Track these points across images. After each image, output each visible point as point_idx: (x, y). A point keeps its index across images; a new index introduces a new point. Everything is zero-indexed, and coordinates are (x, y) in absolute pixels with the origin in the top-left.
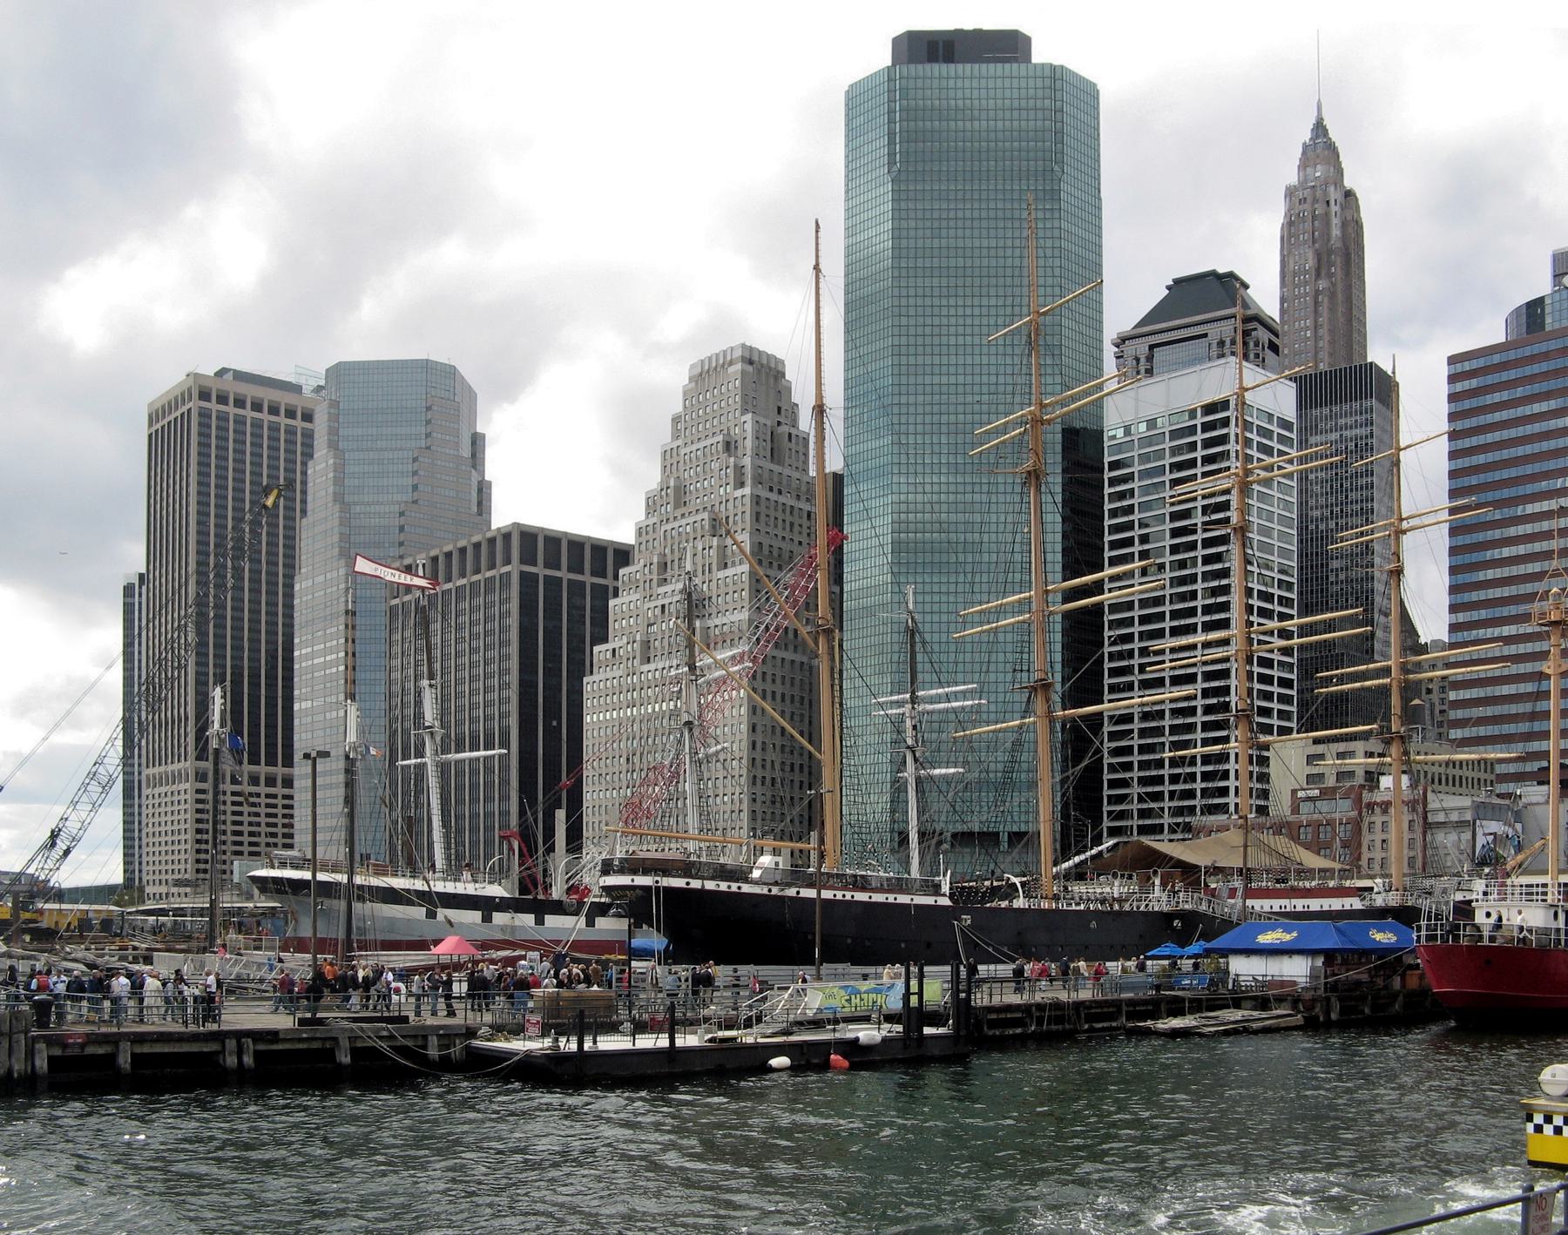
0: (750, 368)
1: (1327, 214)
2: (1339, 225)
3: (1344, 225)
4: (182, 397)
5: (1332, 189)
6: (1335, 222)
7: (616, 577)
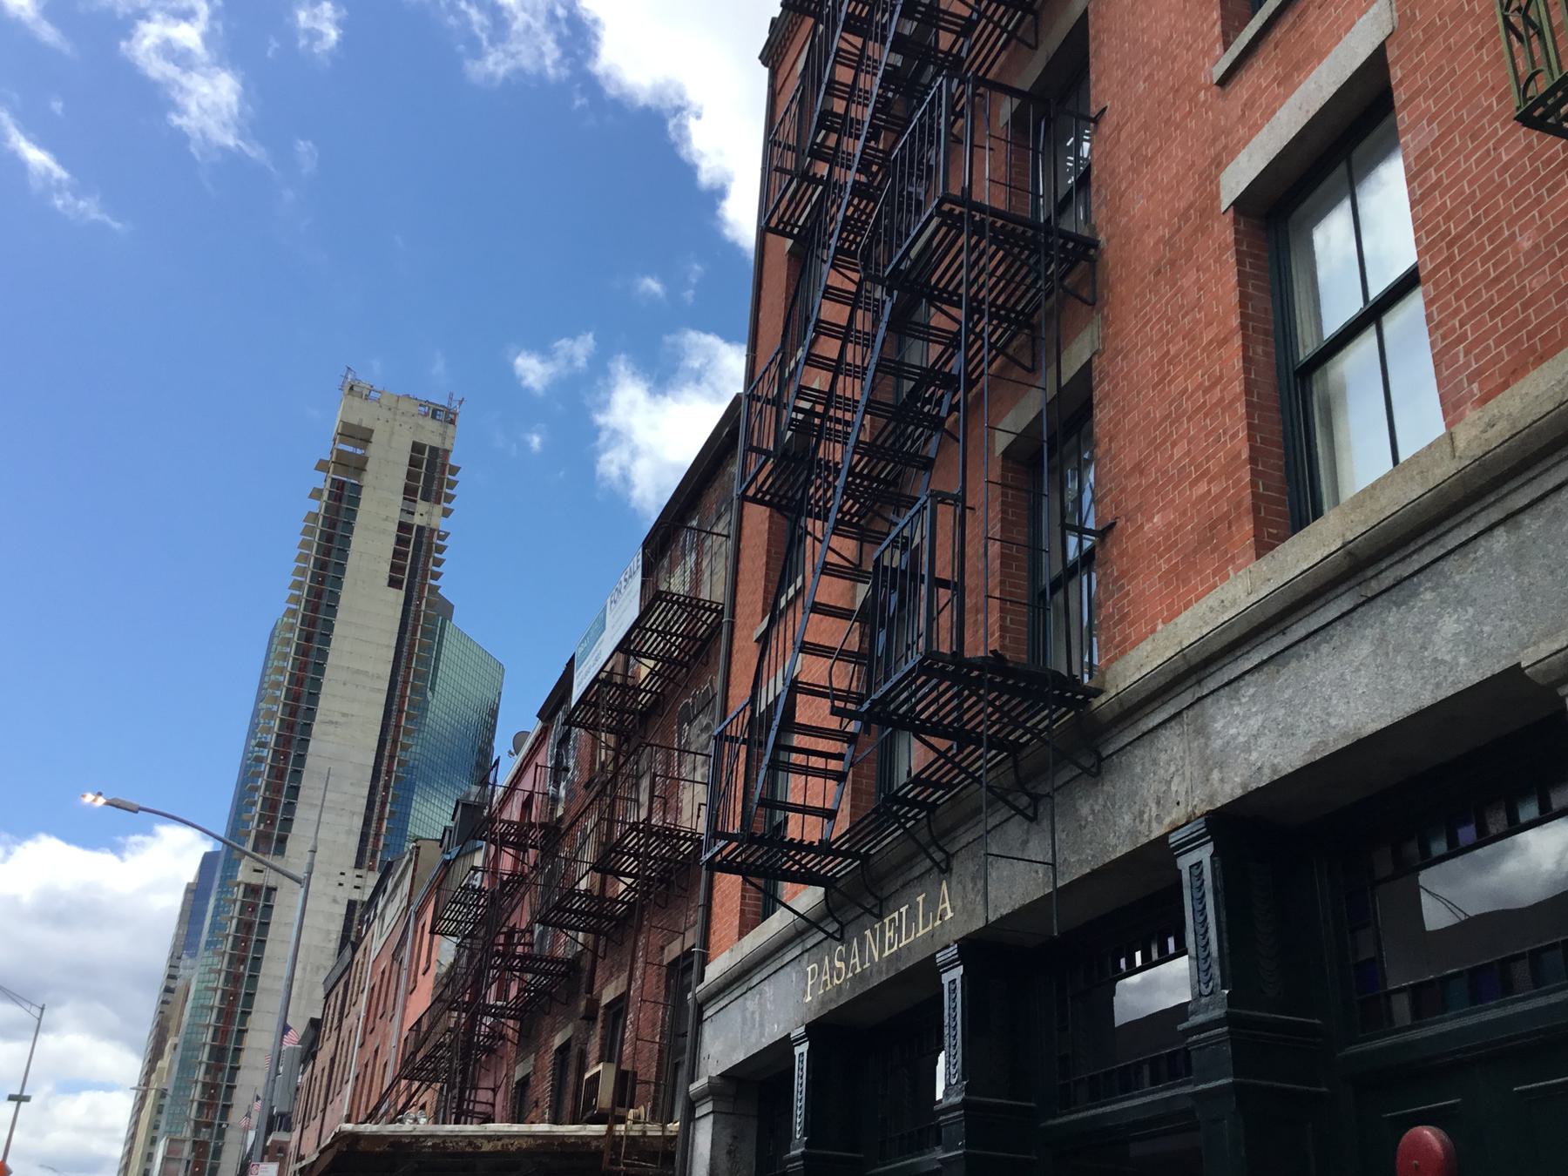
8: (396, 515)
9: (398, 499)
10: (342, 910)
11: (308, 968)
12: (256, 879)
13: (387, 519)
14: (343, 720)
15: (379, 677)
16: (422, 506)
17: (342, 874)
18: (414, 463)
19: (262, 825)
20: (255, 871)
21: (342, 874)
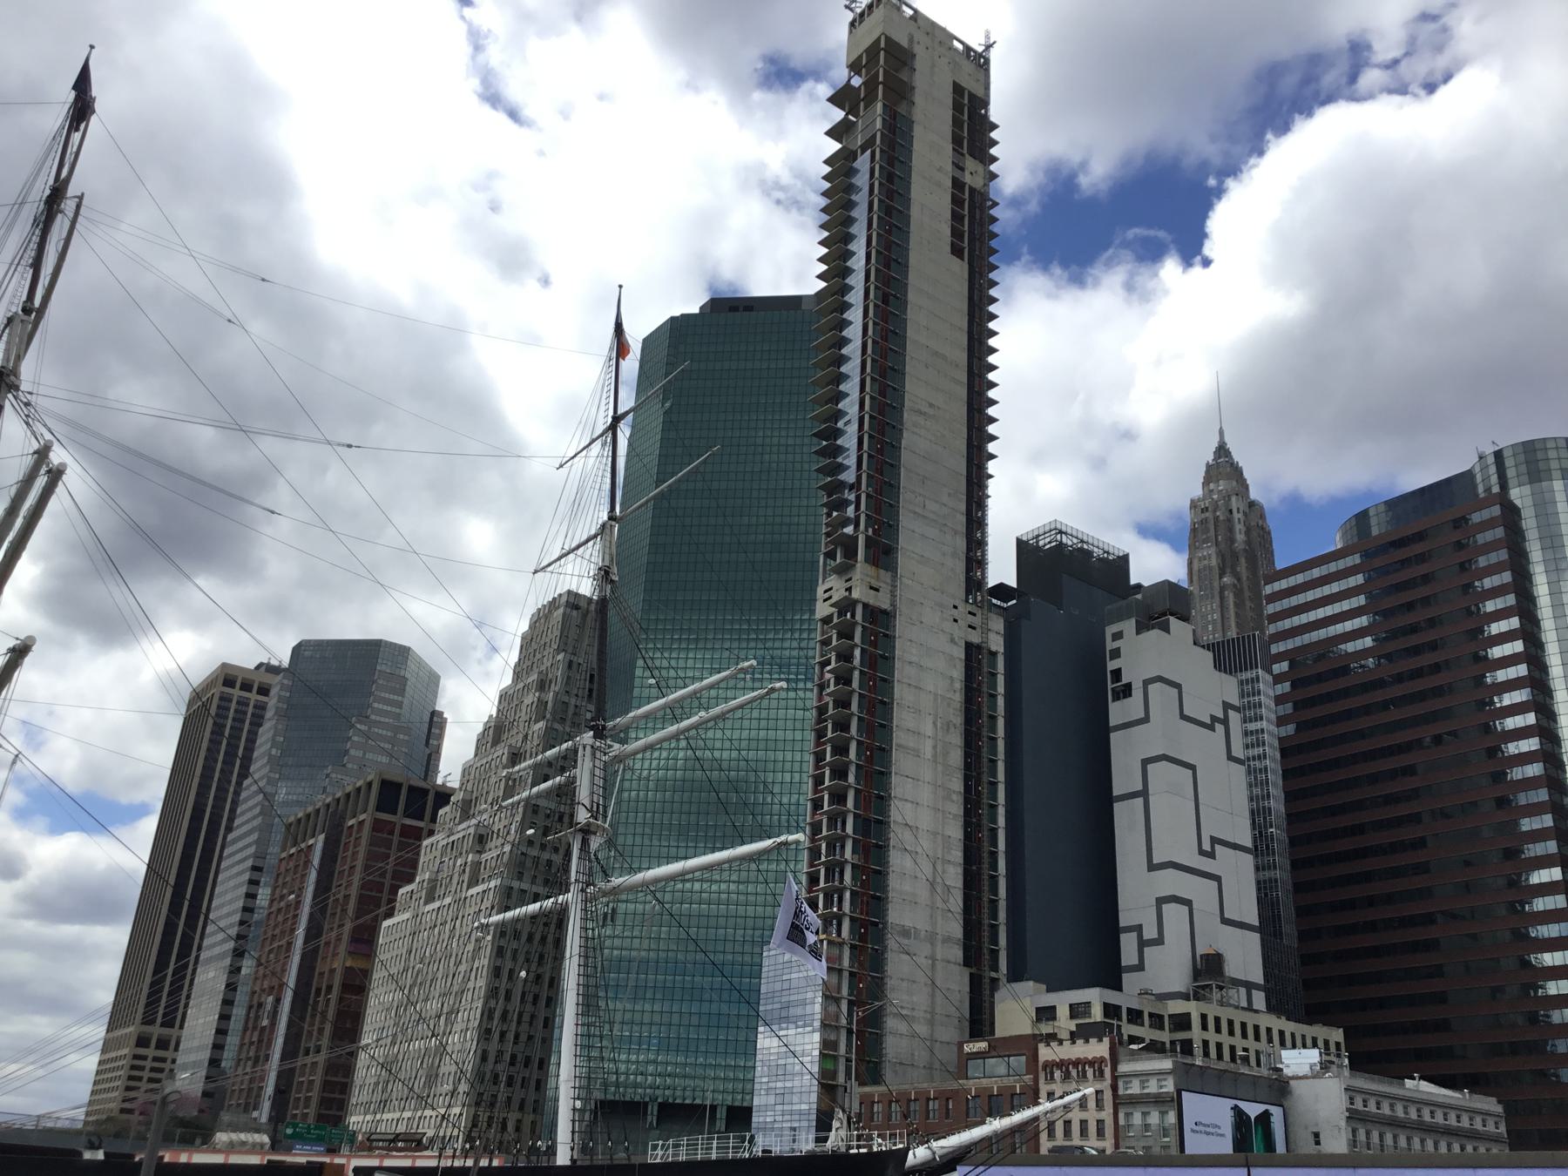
0: (575, 613)
1: (1230, 520)
2: (1244, 529)
3: (1248, 532)
4: (210, 683)
6: (1239, 527)
7: (434, 819)
8: (949, 167)
9: (949, 147)
10: (960, 653)
11: (939, 725)
13: (940, 170)
14: (931, 411)
15: (957, 366)
16: (970, 164)
17: (955, 607)
18: (957, 107)
19: (870, 530)
20: (871, 588)
21: (955, 607)
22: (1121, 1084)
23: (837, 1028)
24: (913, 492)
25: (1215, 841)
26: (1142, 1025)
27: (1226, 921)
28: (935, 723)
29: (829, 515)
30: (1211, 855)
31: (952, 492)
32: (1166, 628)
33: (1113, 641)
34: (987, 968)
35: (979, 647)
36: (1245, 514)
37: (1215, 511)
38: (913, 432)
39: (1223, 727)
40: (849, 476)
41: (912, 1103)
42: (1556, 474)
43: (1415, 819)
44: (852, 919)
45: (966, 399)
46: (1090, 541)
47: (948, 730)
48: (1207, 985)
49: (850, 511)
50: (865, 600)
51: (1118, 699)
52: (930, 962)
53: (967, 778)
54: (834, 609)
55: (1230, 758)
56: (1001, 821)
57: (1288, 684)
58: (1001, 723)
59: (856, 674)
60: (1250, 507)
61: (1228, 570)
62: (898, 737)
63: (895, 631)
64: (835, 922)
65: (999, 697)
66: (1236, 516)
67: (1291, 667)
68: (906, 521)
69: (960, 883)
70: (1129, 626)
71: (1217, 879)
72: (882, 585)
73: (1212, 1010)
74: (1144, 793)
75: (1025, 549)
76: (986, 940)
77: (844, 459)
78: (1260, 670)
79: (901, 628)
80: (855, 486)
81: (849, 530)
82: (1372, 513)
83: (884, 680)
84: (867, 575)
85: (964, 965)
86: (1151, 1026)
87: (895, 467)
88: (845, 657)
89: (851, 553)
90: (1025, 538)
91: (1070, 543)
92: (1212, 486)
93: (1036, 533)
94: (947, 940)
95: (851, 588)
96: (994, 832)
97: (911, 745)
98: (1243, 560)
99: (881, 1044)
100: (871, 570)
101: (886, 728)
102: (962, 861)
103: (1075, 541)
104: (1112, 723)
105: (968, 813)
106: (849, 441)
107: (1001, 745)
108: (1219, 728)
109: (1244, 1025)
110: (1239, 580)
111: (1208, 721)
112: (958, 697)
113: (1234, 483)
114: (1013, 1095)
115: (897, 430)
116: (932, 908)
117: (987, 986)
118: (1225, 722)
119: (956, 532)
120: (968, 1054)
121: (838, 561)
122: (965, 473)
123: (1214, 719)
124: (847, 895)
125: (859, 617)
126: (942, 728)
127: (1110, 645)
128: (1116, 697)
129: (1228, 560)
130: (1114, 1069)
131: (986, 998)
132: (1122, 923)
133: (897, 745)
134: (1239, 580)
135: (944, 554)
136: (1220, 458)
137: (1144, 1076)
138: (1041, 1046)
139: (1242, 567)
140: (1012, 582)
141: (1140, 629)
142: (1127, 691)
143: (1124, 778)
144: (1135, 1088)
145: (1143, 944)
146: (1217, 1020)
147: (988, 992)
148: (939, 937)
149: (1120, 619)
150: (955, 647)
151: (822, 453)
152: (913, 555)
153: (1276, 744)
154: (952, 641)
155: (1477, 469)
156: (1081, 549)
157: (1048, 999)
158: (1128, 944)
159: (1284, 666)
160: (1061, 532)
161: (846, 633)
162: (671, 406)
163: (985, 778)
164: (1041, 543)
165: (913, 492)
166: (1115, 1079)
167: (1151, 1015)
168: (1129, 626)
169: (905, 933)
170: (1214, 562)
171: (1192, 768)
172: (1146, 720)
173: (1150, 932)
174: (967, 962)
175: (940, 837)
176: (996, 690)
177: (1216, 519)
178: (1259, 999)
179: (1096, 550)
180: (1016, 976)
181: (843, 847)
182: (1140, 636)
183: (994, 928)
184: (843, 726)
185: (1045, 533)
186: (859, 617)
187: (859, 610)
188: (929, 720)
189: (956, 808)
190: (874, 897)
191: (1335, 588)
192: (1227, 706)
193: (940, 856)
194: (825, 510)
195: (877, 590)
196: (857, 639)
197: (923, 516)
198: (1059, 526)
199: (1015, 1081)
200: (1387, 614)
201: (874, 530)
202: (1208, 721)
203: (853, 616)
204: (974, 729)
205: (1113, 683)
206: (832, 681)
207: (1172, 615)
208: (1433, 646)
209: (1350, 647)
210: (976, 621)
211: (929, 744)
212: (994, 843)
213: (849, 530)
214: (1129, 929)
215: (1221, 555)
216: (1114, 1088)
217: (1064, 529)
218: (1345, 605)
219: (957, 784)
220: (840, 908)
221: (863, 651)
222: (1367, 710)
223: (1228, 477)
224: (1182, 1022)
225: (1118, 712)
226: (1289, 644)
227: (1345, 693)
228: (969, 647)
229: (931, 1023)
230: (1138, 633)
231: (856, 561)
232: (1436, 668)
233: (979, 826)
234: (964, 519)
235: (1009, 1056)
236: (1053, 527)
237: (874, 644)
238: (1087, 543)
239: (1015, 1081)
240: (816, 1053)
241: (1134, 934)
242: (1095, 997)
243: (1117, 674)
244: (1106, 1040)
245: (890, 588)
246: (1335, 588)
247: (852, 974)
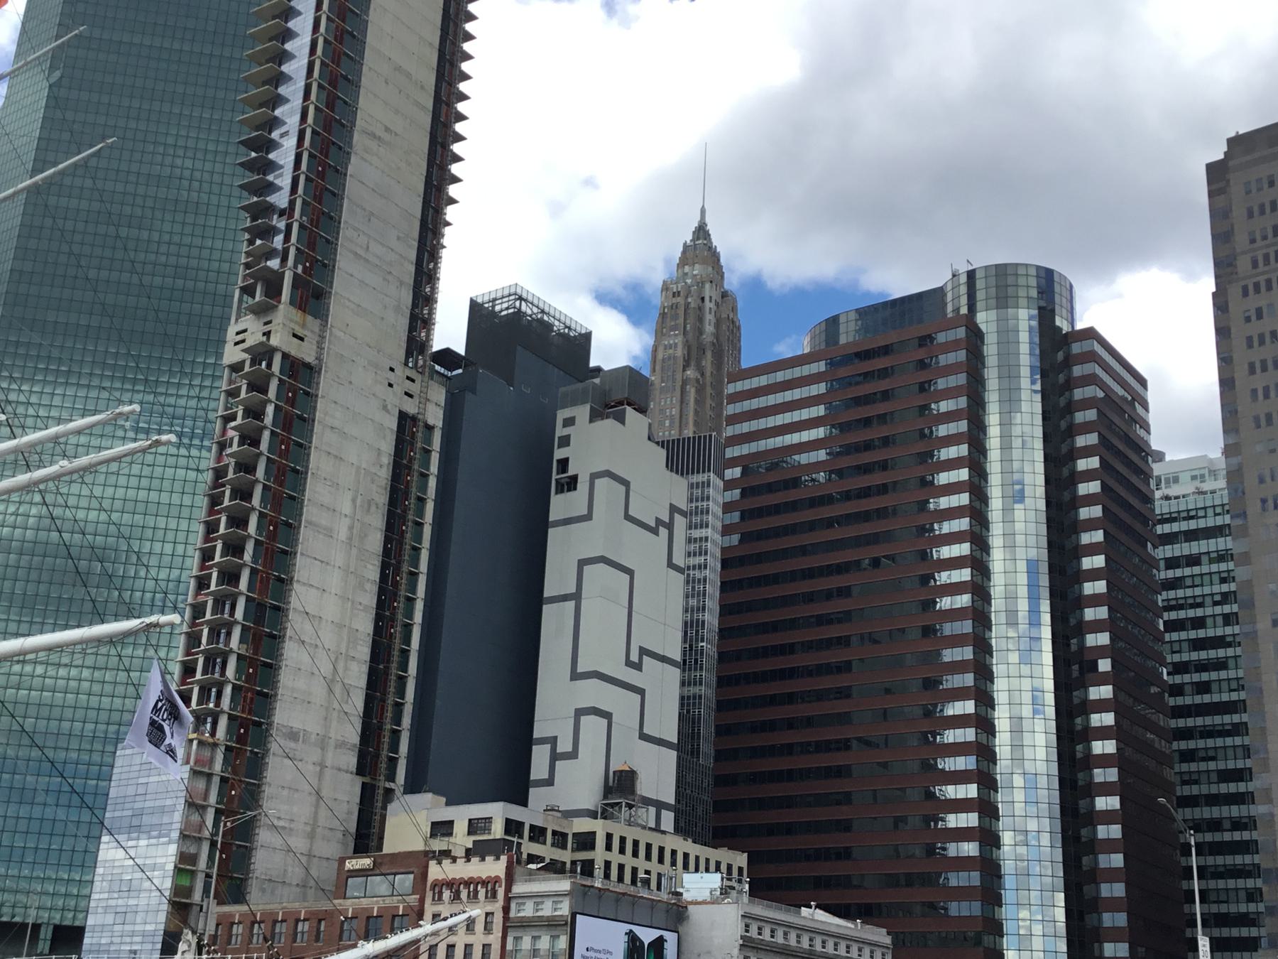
1: (700, 309)
3: (718, 325)
5: (707, 286)
6: (709, 317)
12: (294, 349)
15: (422, 87)
17: (392, 370)
20: (295, 336)
21: (392, 370)
22: (513, 906)
23: (200, 840)
24: (356, 229)
25: (643, 652)
26: (544, 843)
27: (644, 737)
28: (354, 501)
29: (251, 242)
30: (638, 667)
31: (401, 235)
32: (621, 419)
33: (564, 426)
34: (382, 778)
35: (414, 419)
36: (717, 304)
37: (687, 297)
38: (362, 158)
39: (666, 531)
40: (280, 199)
41: (278, 925)
42: (1023, 302)
43: (844, 642)
44: (231, 717)
45: (429, 129)
46: (552, 312)
47: (368, 510)
48: (617, 804)
49: (278, 241)
50: (286, 350)
51: (562, 492)
52: (318, 769)
53: (384, 566)
54: (246, 356)
55: (671, 565)
56: (418, 617)
57: (738, 491)
58: (430, 507)
59: (266, 435)
60: (722, 297)
61: (693, 363)
62: (310, 512)
63: (318, 389)
64: (209, 720)
65: (431, 477)
66: (708, 304)
67: (742, 473)
68: (344, 263)
69: (362, 682)
70: (582, 412)
71: (641, 692)
72: (306, 333)
73: (618, 829)
74: (576, 597)
75: (479, 314)
76: (386, 746)
77: (276, 177)
78: (712, 474)
79: (326, 386)
80: (287, 213)
81: (274, 264)
82: (842, 319)
83: (300, 445)
84: (291, 320)
85: (357, 774)
86: (553, 845)
87: (337, 197)
88: (255, 413)
89: (273, 289)
90: (479, 300)
91: (529, 312)
92: (687, 269)
93: (493, 296)
94: (341, 745)
95: (269, 332)
96: (408, 628)
97: (324, 522)
98: (709, 354)
99: (250, 859)
100: (296, 314)
101: (296, 502)
102: (368, 658)
103: (535, 310)
104: (553, 517)
105: (381, 605)
106: (285, 154)
107: (427, 531)
108: (663, 532)
109: (649, 846)
110: (703, 375)
111: (653, 524)
112: (385, 474)
113: (710, 269)
114: (394, 916)
115: (345, 153)
116: (327, 709)
117: (380, 798)
118: (670, 526)
119: (402, 283)
120: (349, 871)
121: (257, 298)
122: (419, 216)
123: (659, 522)
124: (228, 690)
125: (276, 368)
126: (362, 506)
127: (560, 431)
128: (560, 490)
129: (693, 354)
130: (508, 889)
131: (378, 811)
132: (536, 735)
133: (309, 523)
134: (703, 375)
135: (385, 307)
136: (698, 239)
137: (539, 897)
138: (432, 864)
139: (708, 362)
140: (460, 348)
141: (595, 416)
142: (572, 483)
143: (557, 579)
144: (528, 911)
145: (555, 757)
146: (623, 840)
147: (379, 804)
148: (332, 742)
149: (574, 402)
150: (388, 415)
151: (249, 166)
152: (348, 303)
153: (719, 555)
154: (385, 408)
155: (949, 287)
156: (541, 321)
157: (445, 814)
158: (540, 757)
159: (735, 473)
160: (521, 298)
161: (258, 386)
162: (61, 77)
163: (405, 568)
164: (498, 308)
165: (356, 229)
166: (508, 900)
167: (554, 833)
168: (582, 412)
169: (293, 735)
170: (679, 352)
171: (630, 572)
172: (588, 517)
173: (564, 746)
174: (360, 771)
175: (346, 630)
176: (428, 469)
177: (687, 305)
178: (668, 819)
179: (557, 323)
180: (413, 787)
181: (229, 634)
182: (593, 424)
183: (396, 734)
184: (243, 494)
185: (503, 297)
186: (276, 368)
187: (277, 359)
188: (348, 496)
189: (369, 599)
190: (260, 693)
191: (797, 394)
192: (673, 509)
193: (344, 651)
194: (247, 236)
195: (302, 339)
196: (272, 393)
197: (367, 261)
198: (519, 291)
199: (399, 902)
200: (844, 427)
201: (305, 268)
202: (653, 524)
203: (269, 366)
204: (399, 511)
205: (558, 474)
206: (236, 440)
207: (629, 404)
208: (884, 465)
209: (804, 459)
210: (414, 388)
211: (346, 522)
212: (407, 640)
213: (274, 264)
214: (543, 741)
215: (688, 346)
216: (506, 910)
217: (524, 295)
218: (805, 414)
219: (373, 573)
220: (217, 704)
221: (277, 408)
222: (812, 526)
223: (704, 262)
224: (586, 841)
225: (560, 505)
226: (745, 449)
227: (793, 506)
228: (403, 416)
229: (311, 836)
230: (591, 421)
231: (280, 302)
232: (883, 489)
233: (393, 619)
234: (412, 269)
235: (395, 874)
236: (513, 291)
237: (292, 402)
238: (548, 314)
239: (399, 902)
240: (170, 867)
241: (548, 746)
242: (497, 812)
243: (564, 464)
244: (504, 858)
245: (317, 338)
246: (797, 394)
247: (224, 780)
